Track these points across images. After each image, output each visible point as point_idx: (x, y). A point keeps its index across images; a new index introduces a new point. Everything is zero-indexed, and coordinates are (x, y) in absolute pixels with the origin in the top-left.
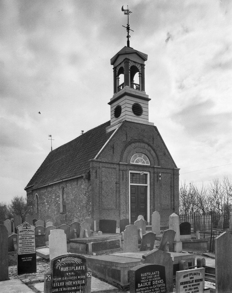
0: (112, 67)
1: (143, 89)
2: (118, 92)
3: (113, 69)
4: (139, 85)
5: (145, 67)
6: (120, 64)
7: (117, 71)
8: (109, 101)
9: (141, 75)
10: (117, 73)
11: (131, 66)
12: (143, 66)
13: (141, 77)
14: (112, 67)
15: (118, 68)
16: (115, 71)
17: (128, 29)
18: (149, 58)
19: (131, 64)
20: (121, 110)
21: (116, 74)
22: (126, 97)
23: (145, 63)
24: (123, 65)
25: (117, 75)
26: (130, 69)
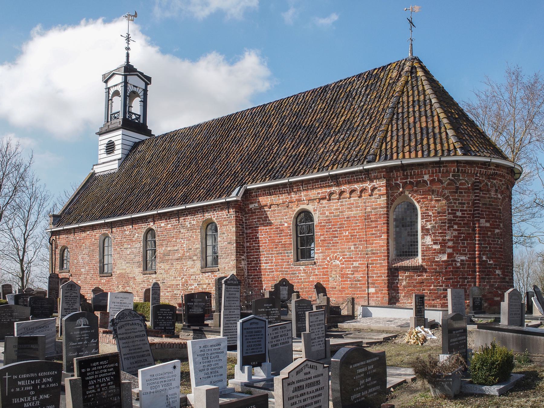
4: (140, 116)
7: (111, 93)
8: (98, 131)
9: (142, 103)
10: (110, 96)
12: (145, 91)
15: (112, 91)
17: (128, 39)
19: (130, 89)
21: (109, 97)
25: (110, 98)
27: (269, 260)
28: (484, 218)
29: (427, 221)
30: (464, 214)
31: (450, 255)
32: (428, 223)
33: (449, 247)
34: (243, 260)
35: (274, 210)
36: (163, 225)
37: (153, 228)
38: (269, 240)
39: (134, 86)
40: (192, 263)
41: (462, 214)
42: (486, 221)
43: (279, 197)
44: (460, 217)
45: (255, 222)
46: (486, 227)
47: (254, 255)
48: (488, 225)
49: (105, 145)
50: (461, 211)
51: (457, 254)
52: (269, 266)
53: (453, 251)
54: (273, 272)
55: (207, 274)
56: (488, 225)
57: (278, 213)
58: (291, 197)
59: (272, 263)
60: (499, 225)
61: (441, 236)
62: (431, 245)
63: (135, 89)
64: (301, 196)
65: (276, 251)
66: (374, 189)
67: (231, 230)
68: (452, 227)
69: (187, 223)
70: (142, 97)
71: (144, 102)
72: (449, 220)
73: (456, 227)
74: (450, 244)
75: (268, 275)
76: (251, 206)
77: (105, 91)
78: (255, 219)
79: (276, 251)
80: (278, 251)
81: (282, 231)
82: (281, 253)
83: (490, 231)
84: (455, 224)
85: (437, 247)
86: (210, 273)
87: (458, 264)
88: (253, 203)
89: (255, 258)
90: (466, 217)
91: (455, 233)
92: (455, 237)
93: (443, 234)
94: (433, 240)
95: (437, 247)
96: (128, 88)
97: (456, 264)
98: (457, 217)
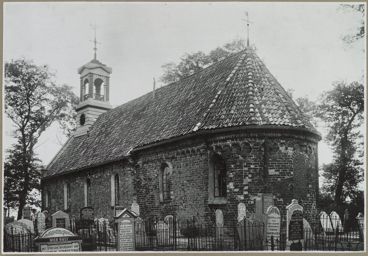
0: (79, 76)
1: (108, 99)
2: (84, 100)
3: (80, 78)
4: (104, 96)
5: (110, 78)
6: (86, 76)
10: (83, 83)
11: (95, 79)
12: (108, 78)
13: (105, 89)
14: (79, 76)
15: (84, 79)
16: (82, 81)
17: (95, 42)
18: (113, 71)
19: (95, 77)
20: (85, 120)
22: (90, 109)
23: (110, 75)
24: (87, 77)
26: (94, 82)
27: (149, 200)
28: (274, 168)
29: (230, 172)
30: (257, 166)
31: (246, 196)
32: (231, 173)
33: (245, 190)
34: (135, 199)
36: (94, 176)
39: (99, 75)
41: (255, 166)
42: (275, 171)
44: (253, 169)
46: (275, 175)
48: (277, 173)
49: (80, 118)
50: (254, 164)
51: (252, 195)
53: (249, 193)
56: (277, 173)
58: (158, 157)
60: (290, 173)
61: (240, 183)
62: (233, 189)
63: (99, 77)
64: (162, 156)
66: (198, 150)
68: (248, 176)
69: (105, 175)
70: (105, 82)
71: (107, 86)
72: (245, 171)
73: (250, 176)
74: (246, 188)
77: (80, 79)
78: (141, 171)
83: (280, 178)
84: (250, 173)
85: (237, 190)
87: (252, 202)
90: (258, 169)
91: (249, 180)
92: (249, 183)
93: (242, 181)
94: (234, 185)
95: (237, 190)
96: (94, 77)
97: (250, 203)
98: (251, 169)
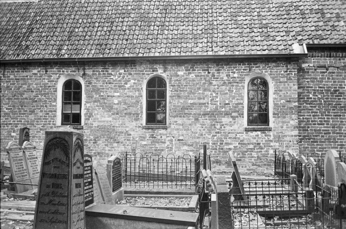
35: (333, 73)
36: (180, 73)
37: (164, 75)
38: (324, 101)
40: (231, 119)
43: (340, 60)
45: (308, 82)
47: (304, 116)
52: (324, 127)
54: (329, 133)
55: (255, 133)
57: (337, 76)
59: (328, 124)
65: (334, 113)
67: (291, 88)
75: (322, 136)
76: (304, 66)
79: (334, 113)
80: (336, 113)
81: (342, 93)
82: (340, 116)
86: (259, 133)
88: (307, 63)
89: (306, 118)
